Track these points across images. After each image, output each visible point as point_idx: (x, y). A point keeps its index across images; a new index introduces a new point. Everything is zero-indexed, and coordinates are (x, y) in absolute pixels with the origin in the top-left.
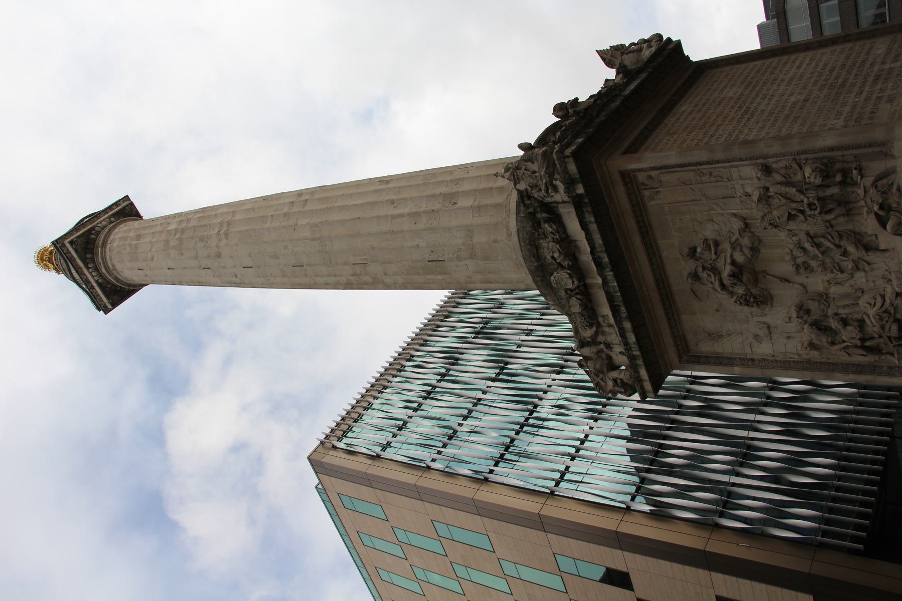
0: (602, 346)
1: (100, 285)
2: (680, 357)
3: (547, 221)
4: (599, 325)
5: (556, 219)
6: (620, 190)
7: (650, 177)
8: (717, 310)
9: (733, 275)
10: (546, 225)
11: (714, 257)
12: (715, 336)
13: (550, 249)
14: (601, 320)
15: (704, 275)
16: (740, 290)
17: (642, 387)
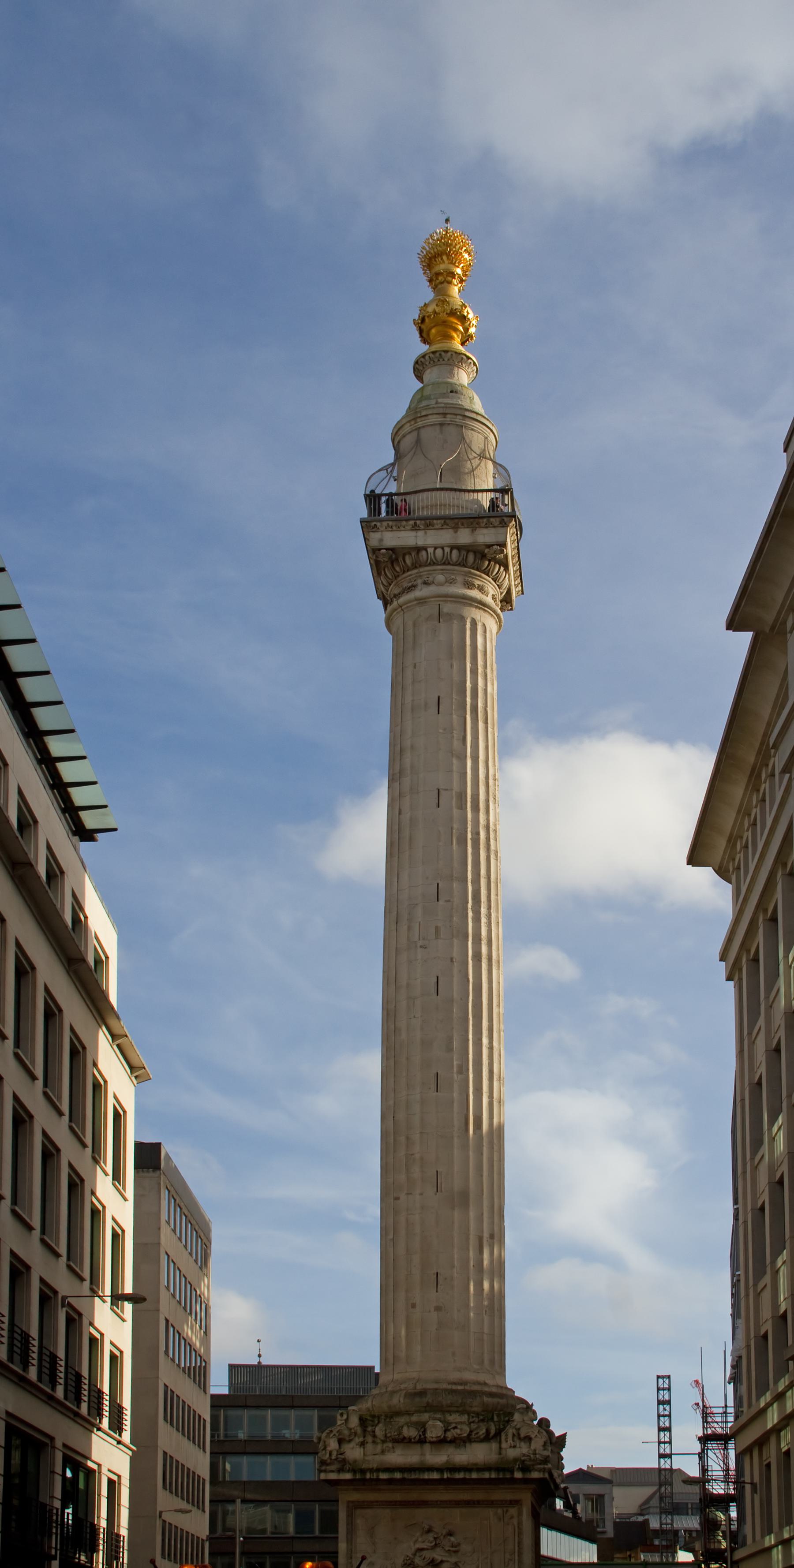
0: (361, 1439)
1: (418, 549)
2: (353, 1502)
3: (488, 1431)
4: (383, 1442)
5: (487, 1438)
6: (509, 1496)
7: (512, 1517)
8: (395, 1539)
9: (433, 1560)
10: (484, 1431)
11: (447, 1549)
12: (371, 1532)
13: (461, 1424)
14: (390, 1445)
15: (431, 1536)
16: (417, 1561)
17: (332, 1471)
